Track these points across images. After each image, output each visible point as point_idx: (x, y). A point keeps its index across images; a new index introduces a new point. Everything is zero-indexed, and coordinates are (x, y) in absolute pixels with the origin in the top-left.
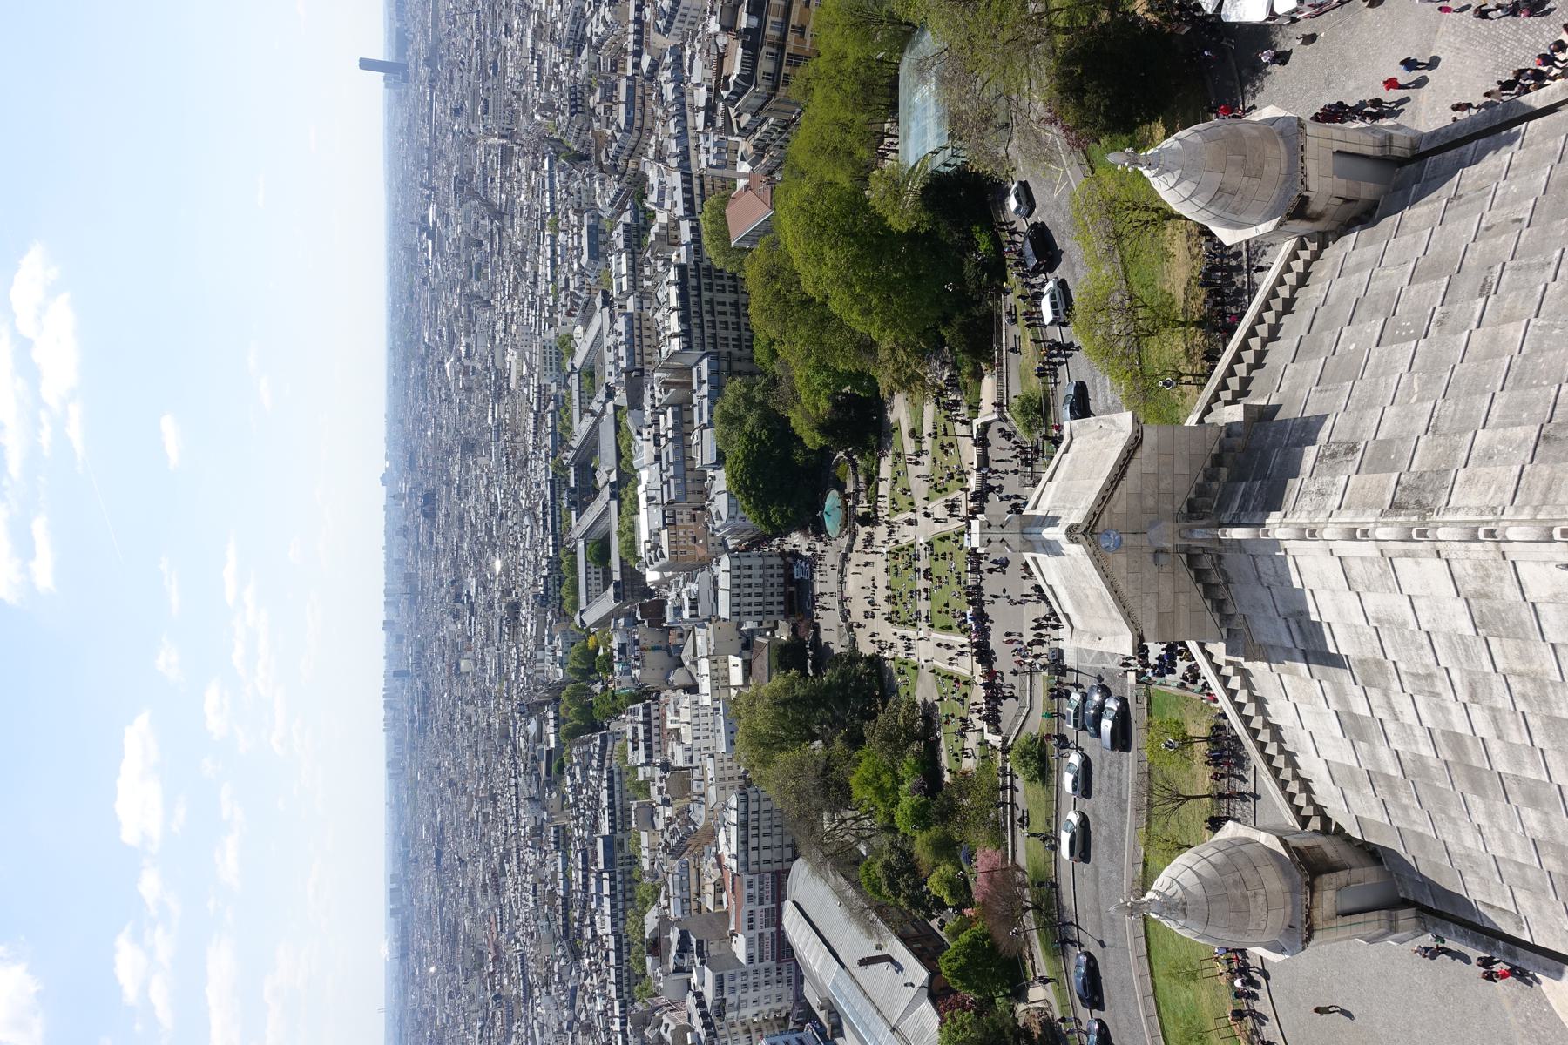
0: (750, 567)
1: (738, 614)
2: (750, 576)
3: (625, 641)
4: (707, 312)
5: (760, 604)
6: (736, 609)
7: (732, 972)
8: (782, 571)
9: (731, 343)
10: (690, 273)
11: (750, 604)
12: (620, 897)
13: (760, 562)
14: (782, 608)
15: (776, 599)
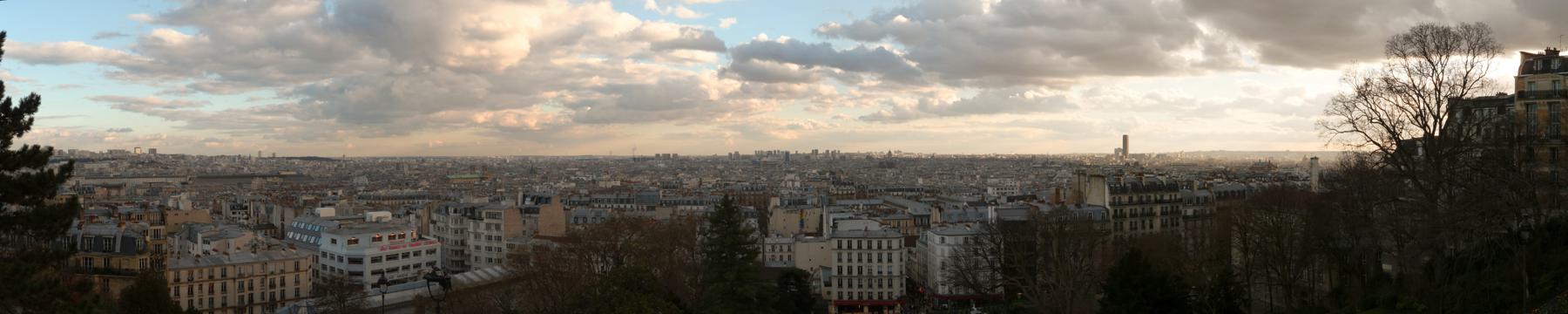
0: (890, 260)
1: (840, 247)
2: (880, 260)
3: (809, 202)
4: (1143, 209)
5: (850, 270)
6: (845, 244)
7: (502, 227)
8: (885, 297)
9: (1119, 233)
10: (1173, 195)
11: (850, 260)
12: (615, 206)
13: (896, 272)
14: (846, 297)
15: (855, 290)
